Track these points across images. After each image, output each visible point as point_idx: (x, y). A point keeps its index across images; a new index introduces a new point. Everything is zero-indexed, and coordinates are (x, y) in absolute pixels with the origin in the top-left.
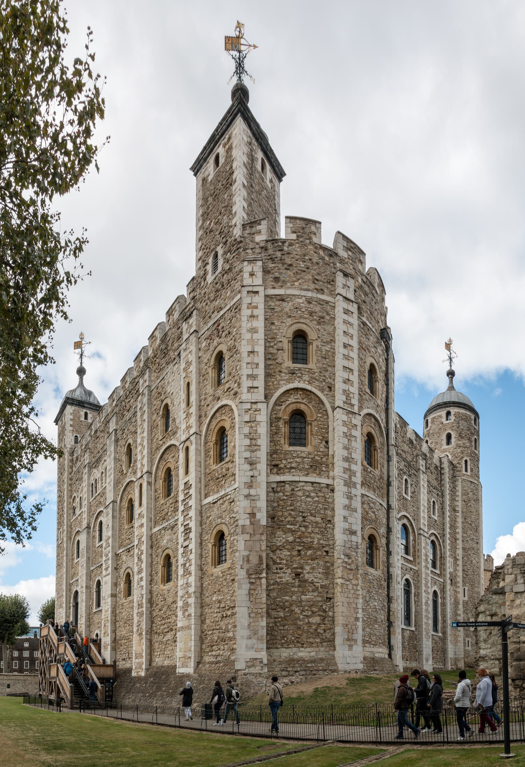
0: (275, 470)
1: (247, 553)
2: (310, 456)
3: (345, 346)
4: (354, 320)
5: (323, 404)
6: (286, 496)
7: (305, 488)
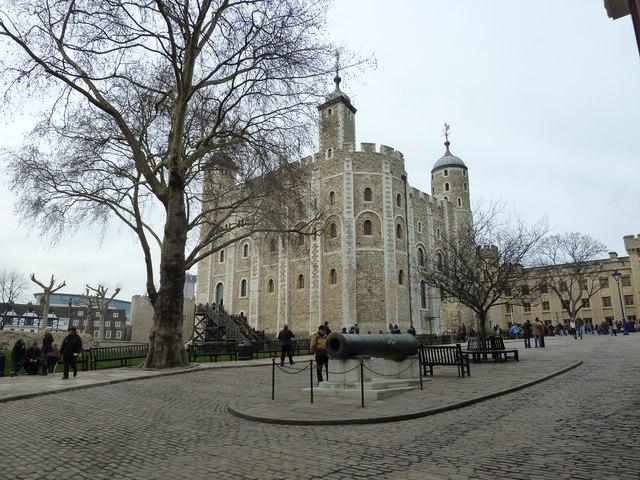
4: (390, 181)
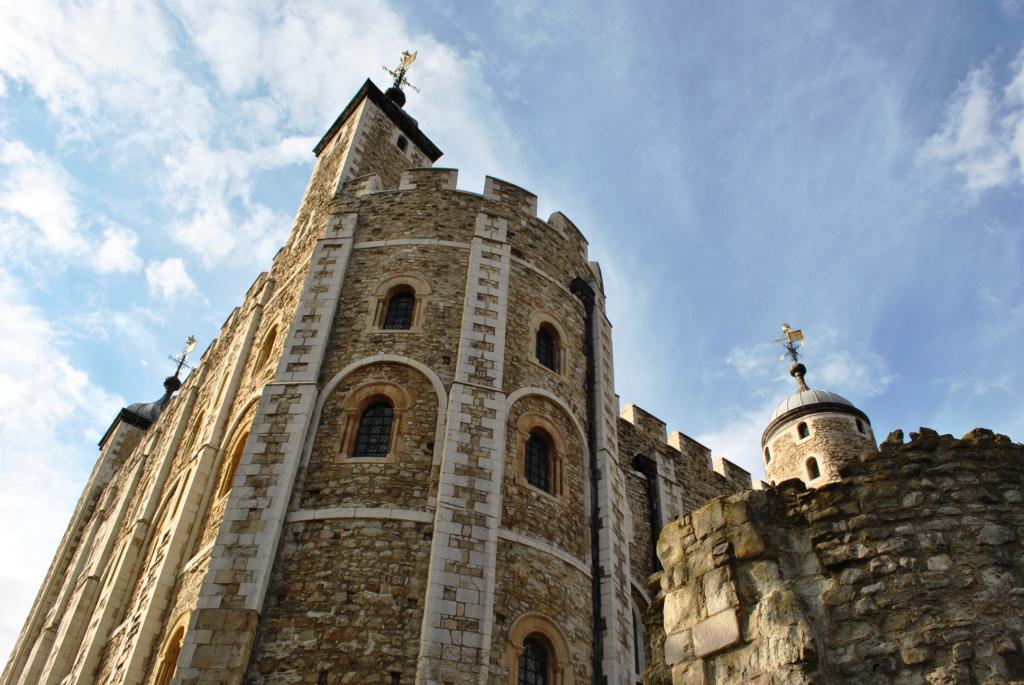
0: (311, 501)
1: (195, 673)
2: (389, 472)
3: (480, 297)
4: (505, 264)
5: (429, 382)
6: (321, 548)
7: (364, 531)
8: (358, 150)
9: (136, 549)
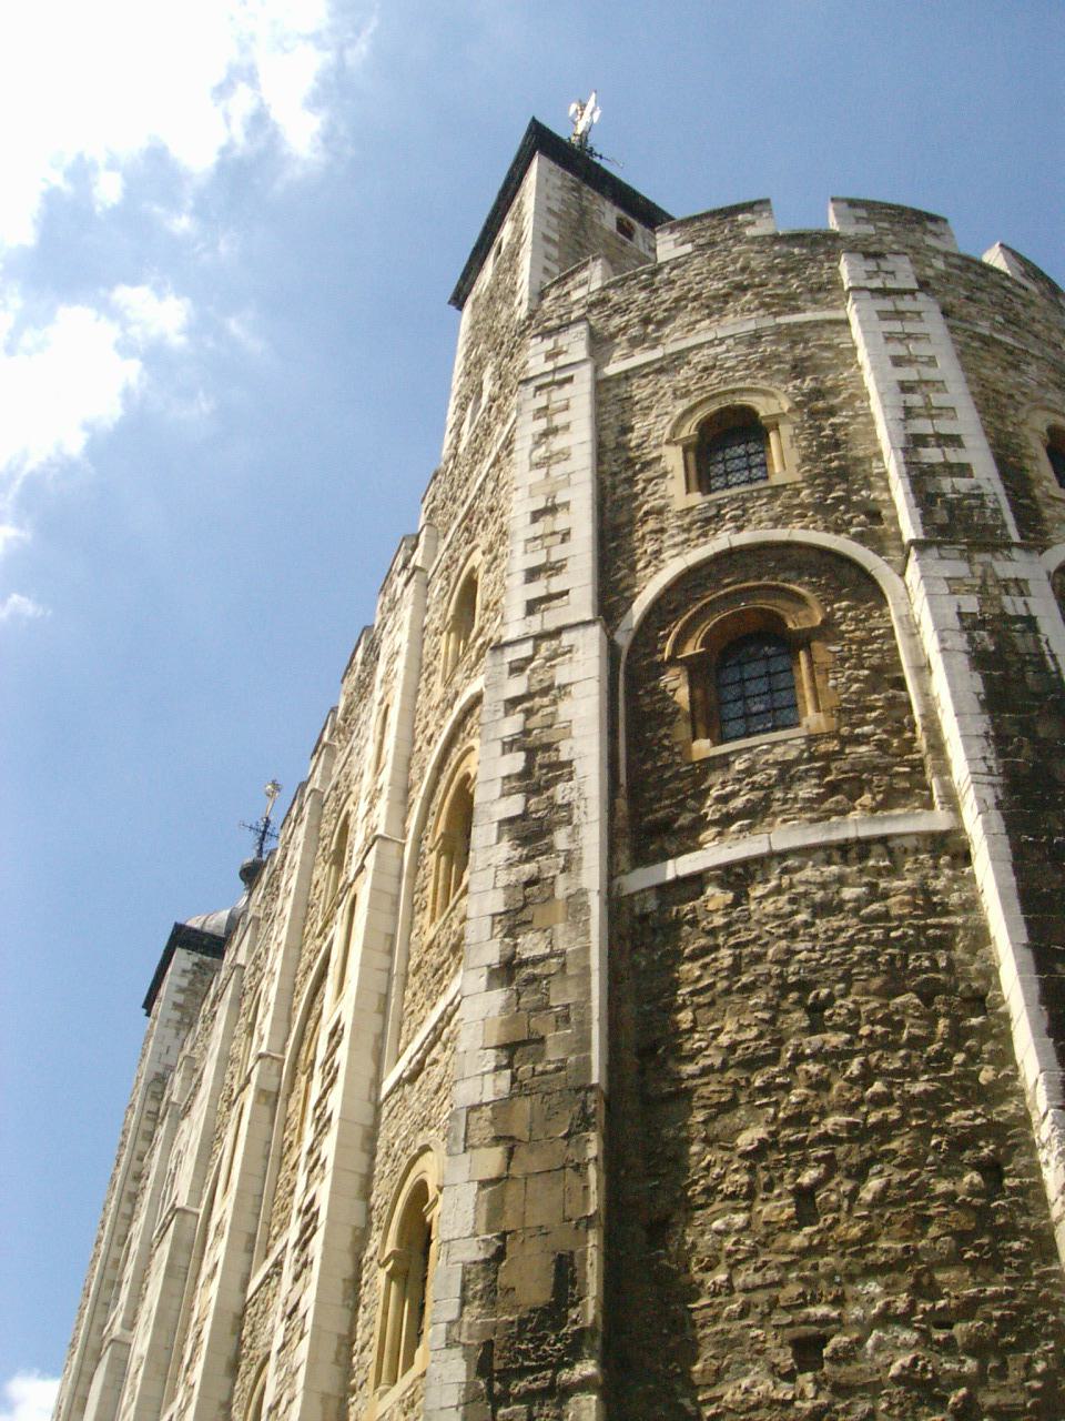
8: (547, 239)
9: (265, 1111)
